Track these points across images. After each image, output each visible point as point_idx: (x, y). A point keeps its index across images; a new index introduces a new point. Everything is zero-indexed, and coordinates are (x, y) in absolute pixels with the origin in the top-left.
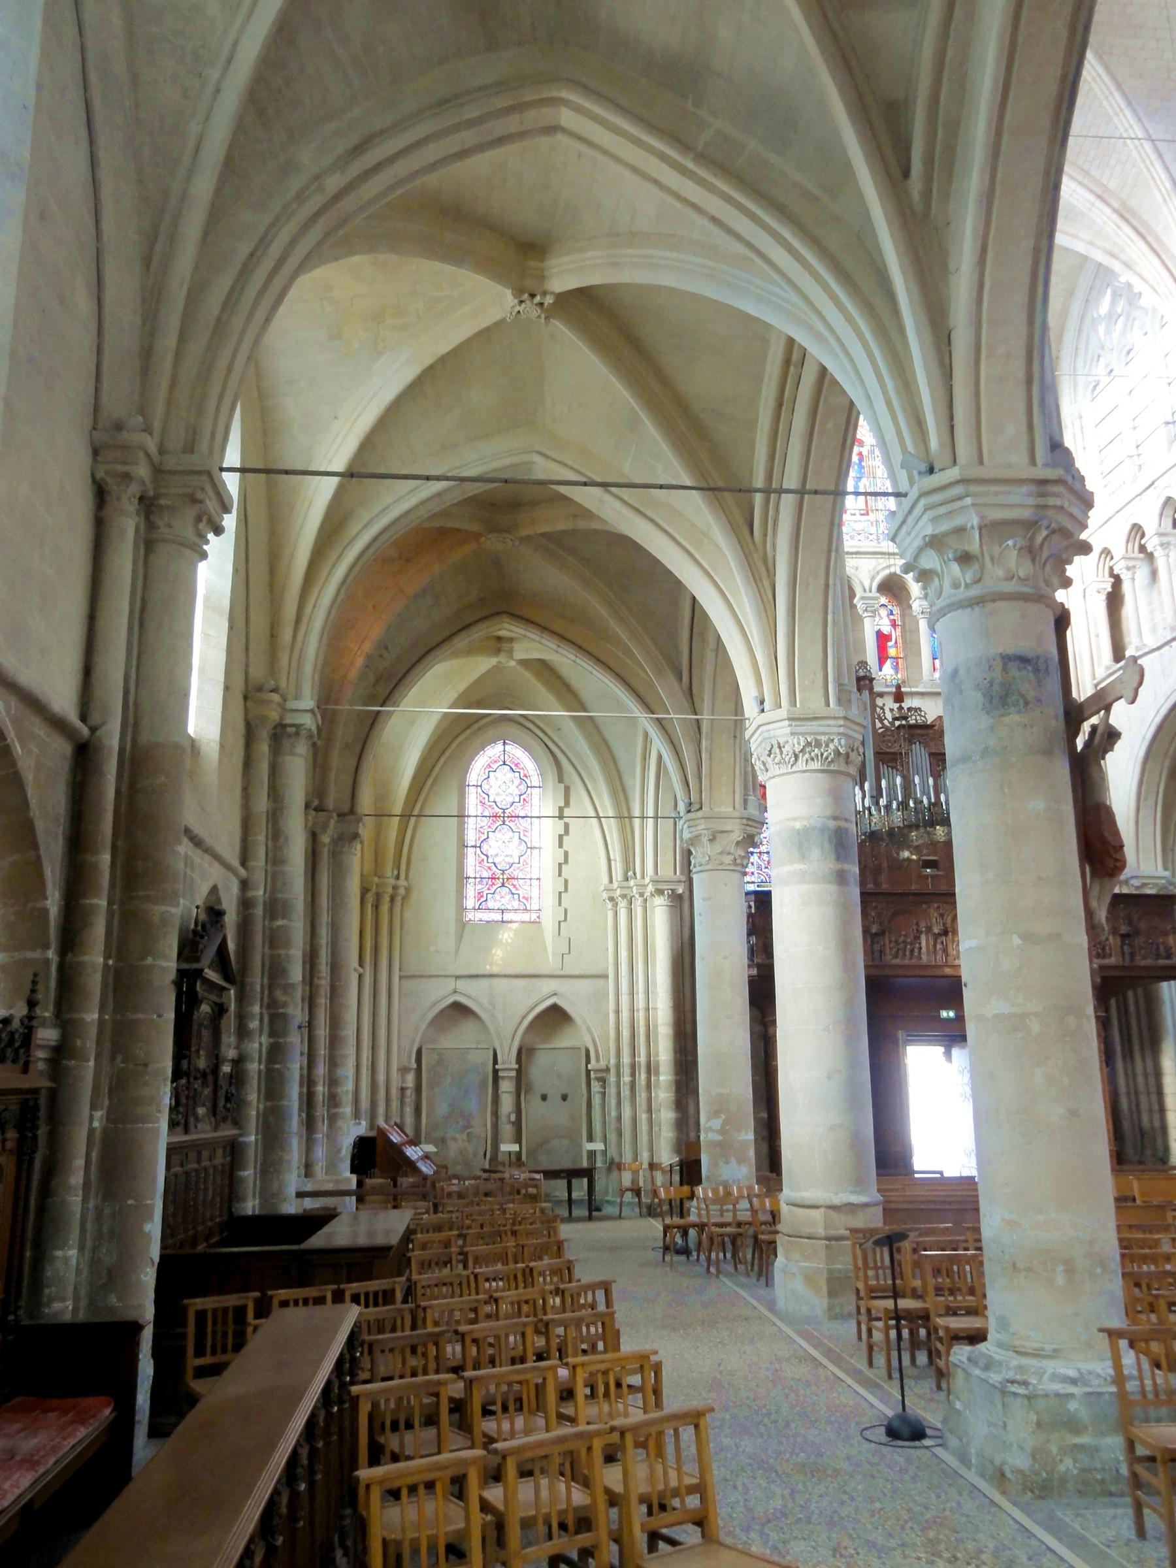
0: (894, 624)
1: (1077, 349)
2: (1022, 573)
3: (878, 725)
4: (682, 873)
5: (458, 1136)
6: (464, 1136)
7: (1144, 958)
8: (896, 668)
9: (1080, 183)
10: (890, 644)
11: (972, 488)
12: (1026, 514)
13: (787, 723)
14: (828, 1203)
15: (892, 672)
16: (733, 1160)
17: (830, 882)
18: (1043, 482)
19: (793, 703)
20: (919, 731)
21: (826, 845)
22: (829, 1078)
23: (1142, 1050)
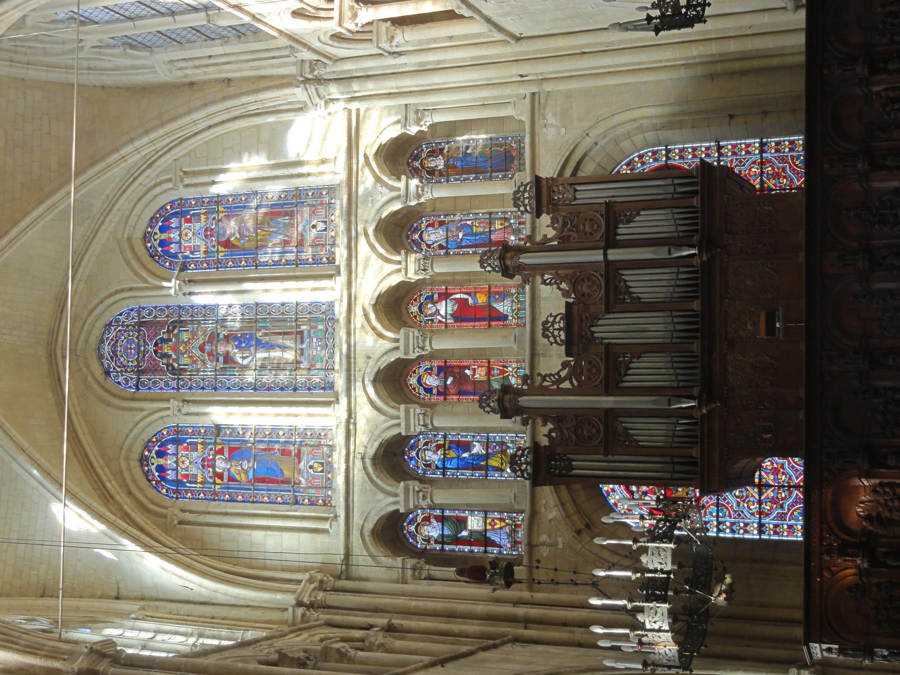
0: (445, 296)
1: (89, 69)
3: (566, 385)
10: (470, 301)
15: (507, 302)
20: (576, 328)
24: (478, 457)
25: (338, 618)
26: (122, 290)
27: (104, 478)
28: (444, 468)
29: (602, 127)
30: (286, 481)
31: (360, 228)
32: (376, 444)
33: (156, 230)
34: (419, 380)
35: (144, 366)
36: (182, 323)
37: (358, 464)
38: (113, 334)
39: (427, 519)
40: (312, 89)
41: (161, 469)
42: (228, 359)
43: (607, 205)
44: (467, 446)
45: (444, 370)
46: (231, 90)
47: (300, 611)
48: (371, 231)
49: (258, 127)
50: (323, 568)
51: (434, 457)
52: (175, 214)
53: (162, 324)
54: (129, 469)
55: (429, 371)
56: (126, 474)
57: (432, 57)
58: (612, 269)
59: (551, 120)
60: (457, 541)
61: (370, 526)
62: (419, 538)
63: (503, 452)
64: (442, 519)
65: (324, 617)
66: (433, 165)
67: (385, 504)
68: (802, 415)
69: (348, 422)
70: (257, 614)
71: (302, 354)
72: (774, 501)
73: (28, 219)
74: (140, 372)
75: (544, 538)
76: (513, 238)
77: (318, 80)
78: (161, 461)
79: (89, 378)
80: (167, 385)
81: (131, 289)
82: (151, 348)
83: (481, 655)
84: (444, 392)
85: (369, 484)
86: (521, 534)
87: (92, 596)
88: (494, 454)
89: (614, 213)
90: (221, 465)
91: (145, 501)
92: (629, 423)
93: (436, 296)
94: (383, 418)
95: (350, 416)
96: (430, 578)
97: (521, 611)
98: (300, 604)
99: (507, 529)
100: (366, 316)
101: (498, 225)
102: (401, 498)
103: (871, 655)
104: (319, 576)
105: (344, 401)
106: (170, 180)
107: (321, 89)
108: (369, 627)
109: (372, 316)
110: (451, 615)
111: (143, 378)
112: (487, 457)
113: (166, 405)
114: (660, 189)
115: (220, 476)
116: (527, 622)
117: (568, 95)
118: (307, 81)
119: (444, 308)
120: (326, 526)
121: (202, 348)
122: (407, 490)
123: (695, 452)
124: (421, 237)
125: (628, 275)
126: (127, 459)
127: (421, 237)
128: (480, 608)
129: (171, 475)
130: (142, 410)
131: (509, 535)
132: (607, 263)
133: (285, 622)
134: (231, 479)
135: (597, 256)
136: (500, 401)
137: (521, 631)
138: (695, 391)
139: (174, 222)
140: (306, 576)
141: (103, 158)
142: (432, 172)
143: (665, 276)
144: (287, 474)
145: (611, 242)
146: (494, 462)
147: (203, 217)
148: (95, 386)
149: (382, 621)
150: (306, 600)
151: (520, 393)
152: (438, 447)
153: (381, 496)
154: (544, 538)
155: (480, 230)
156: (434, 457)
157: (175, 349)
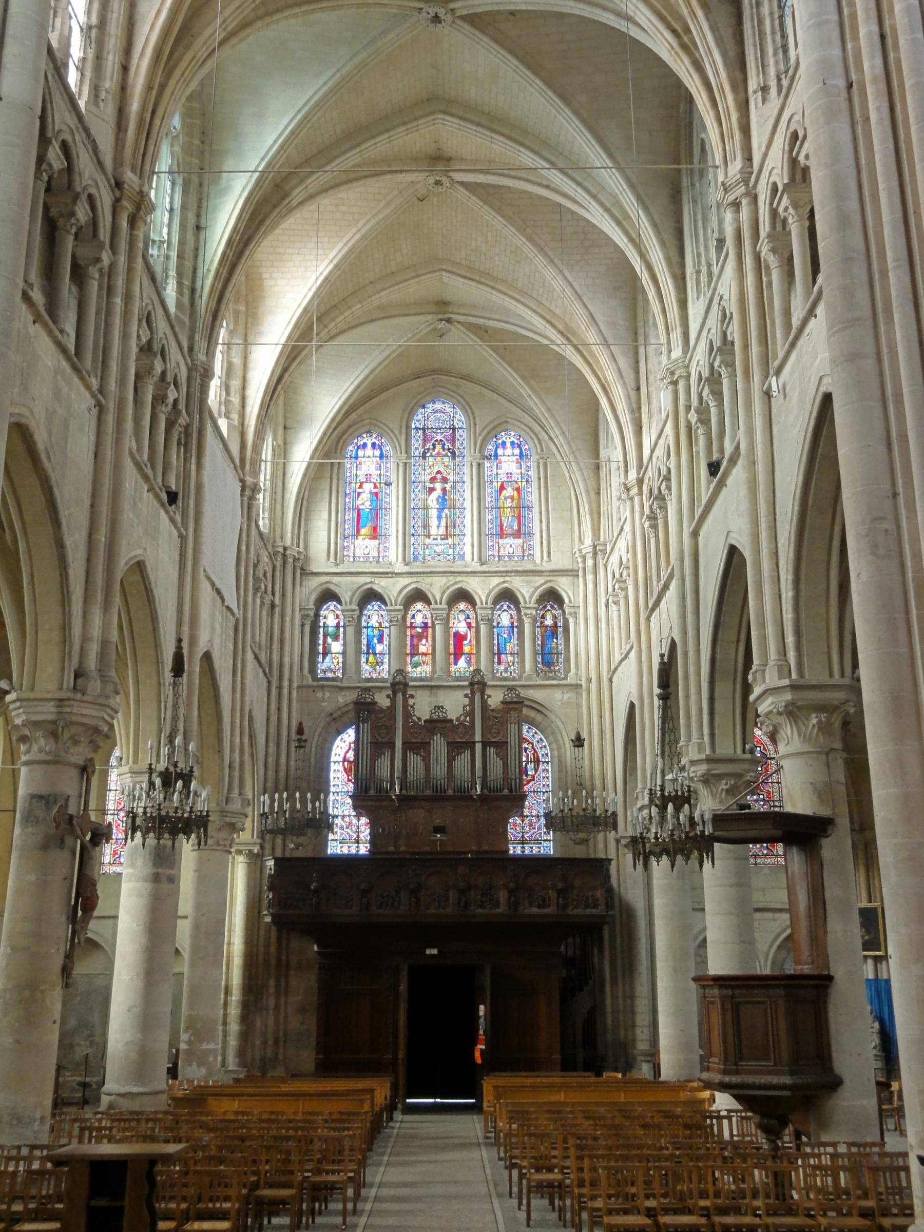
0: (469, 626)
2: (47, 749)
4: (258, 837)
5: (82, 1043)
6: (87, 1043)
7: (576, 907)
8: (469, 663)
9: (535, 311)
10: (465, 642)
11: (25, 704)
12: (52, 717)
13: (129, 775)
14: (117, 1092)
15: (465, 665)
16: (195, 1063)
17: (146, 881)
18: (61, 700)
19: (136, 761)
20: (439, 725)
21: (147, 857)
22: (129, 1010)
23: (624, 978)
24: (374, 649)
25: (278, 573)
26: (474, 418)
27: (358, 411)
28: (368, 627)
29: (561, 726)
30: (358, 531)
31: (507, 579)
32: (380, 591)
33: (512, 439)
34: (419, 611)
35: (428, 432)
36: (454, 456)
37: (368, 580)
38: (448, 410)
39: (338, 617)
40: (590, 549)
41: (364, 446)
42: (432, 490)
43: (507, 742)
44: (381, 640)
45: (425, 626)
46: (593, 495)
47: (281, 550)
48: (506, 585)
49: (571, 510)
50: (307, 559)
51: (374, 622)
52: (521, 452)
53: (453, 444)
54: (366, 425)
55: (425, 617)
56: (360, 424)
57: (603, 625)
58: (471, 745)
59: (566, 696)
60: (325, 636)
61: (332, 587)
62: (326, 612)
63: (377, 664)
64: (338, 626)
65: (278, 564)
66: (548, 617)
67: (345, 596)
68: (391, 849)
69: (392, 573)
70: (279, 521)
71: (435, 539)
72: (350, 823)
73: (512, 372)
74: (424, 429)
75: (327, 694)
76: (503, 668)
77: (595, 554)
78: (369, 446)
79: (419, 397)
80: (417, 449)
81: (475, 424)
82: (439, 437)
83: (261, 671)
84: (412, 627)
85: (356, 586)
86: (330, 675)
87: (285, 411)
88: (376, 658)
89: (501, 746)
90: (368, 487)
91: (344, 438)
92: (388, 754)
93: (469, 620)
94: (395, 595)
95: (397, 574)
96: (303, 625)
97: (286, 684)
98: (285, 549)
99: (332, 667)
100: (456, 583)
101: (510, 659)
102: (349, 607)
103: (270, 889)
104: (302, 557)
105: (406, 569)
106: (542, 450)
107: (591, 555)
108: (273, 594)
109: (456, 587)
110: (282, 641)
111: (421, 432)
112: (374, 654)
113: (403, 451)
114: (513, 772)
115: (361, 487)
116: (280, 687)
117: (579, 706)
118: (595, 547)
119: (462, 628)
120: (332, 560)
121: (439, 472)
122: (353, 611)
123: (372, 792)
124: (505, 610)
125: (468, 753)
126: (370, 423)
127: (505, 610)
128: (287, 660)
129: (361, 453)
130: (400, 434)
131: (329, 668)
132: (474, 743)
133: (275, 542)
134: (359, 494)
135: (478, 737)
136: (399, 683)
137: (274, 685)
138: (404, 792)
139: (517, 451)
140: (301, 549)
141: (553, 416)
142: (543, 617)
143: (467, 775)
144: (363, 531)
145: (485, 744)
146: (371, 658)
147: (519, 471)
148: (415, 401)
149: (277, 602)
150: (288, 552)
151: (404, 694)
152: (380, 624)
153: (350, 594)
154: (327, 694)
155: (508, 648)
156: (374, 622)
157: (438, 454)
